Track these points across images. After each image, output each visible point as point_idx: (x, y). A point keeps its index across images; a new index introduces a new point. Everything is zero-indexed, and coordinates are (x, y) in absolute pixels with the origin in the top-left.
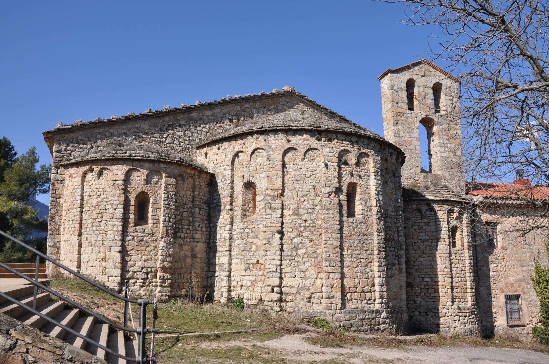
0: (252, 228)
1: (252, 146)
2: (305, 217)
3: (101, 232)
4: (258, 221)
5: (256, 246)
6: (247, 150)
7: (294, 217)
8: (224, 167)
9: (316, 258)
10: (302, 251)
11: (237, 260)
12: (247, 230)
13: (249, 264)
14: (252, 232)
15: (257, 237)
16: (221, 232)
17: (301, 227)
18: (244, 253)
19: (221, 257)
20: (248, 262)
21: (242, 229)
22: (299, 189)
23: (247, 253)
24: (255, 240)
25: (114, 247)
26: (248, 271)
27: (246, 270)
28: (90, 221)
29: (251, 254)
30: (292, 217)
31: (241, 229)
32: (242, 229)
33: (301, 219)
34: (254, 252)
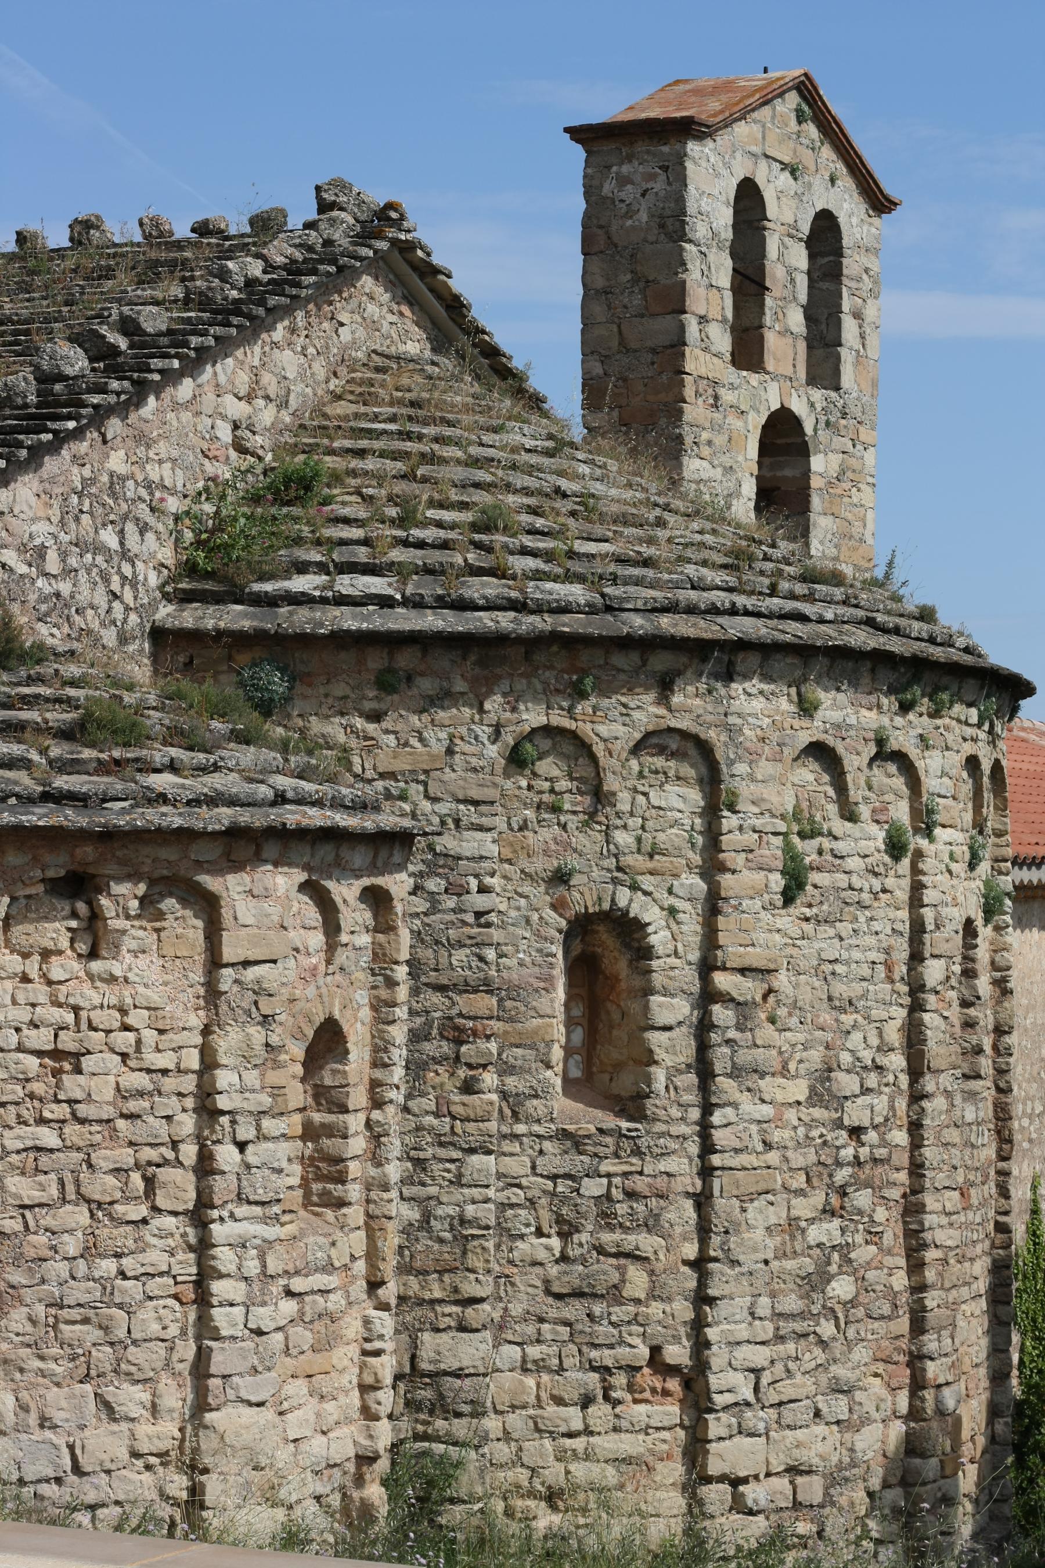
0: (626, 1175)
1: (636, 715)
2: (856, 1113)
3: (154, 1286)
4: (662, 1135)
5: (652, 1273)
6: (603, 730)
7: (818, 1113)
8: (443, 808)
9: (889, 1318)
10: (842, 1288)
11: (534, 1352)
12: (594, 1187)
13: (605, 1371)
14: (631, 1195)
15: (651, 1224)
16: (433, 1190)
17: (839, 1164)
18: (574, 1310)
19: (426, 1337)
20: (606, 1357)
21: (568, 1176)
22: (840, 969)
23: (598, 1309)
24: (646, 1242)
25: (240, 1374)
26: (600, 1411)
27: (586, 1402)
28: (81, 1216)
29: (619, 1313)
30: (805, 1112)
31: (554, 1178)
32: (568, 1176)
33: (838, 1124)
34: (637, 1301)
